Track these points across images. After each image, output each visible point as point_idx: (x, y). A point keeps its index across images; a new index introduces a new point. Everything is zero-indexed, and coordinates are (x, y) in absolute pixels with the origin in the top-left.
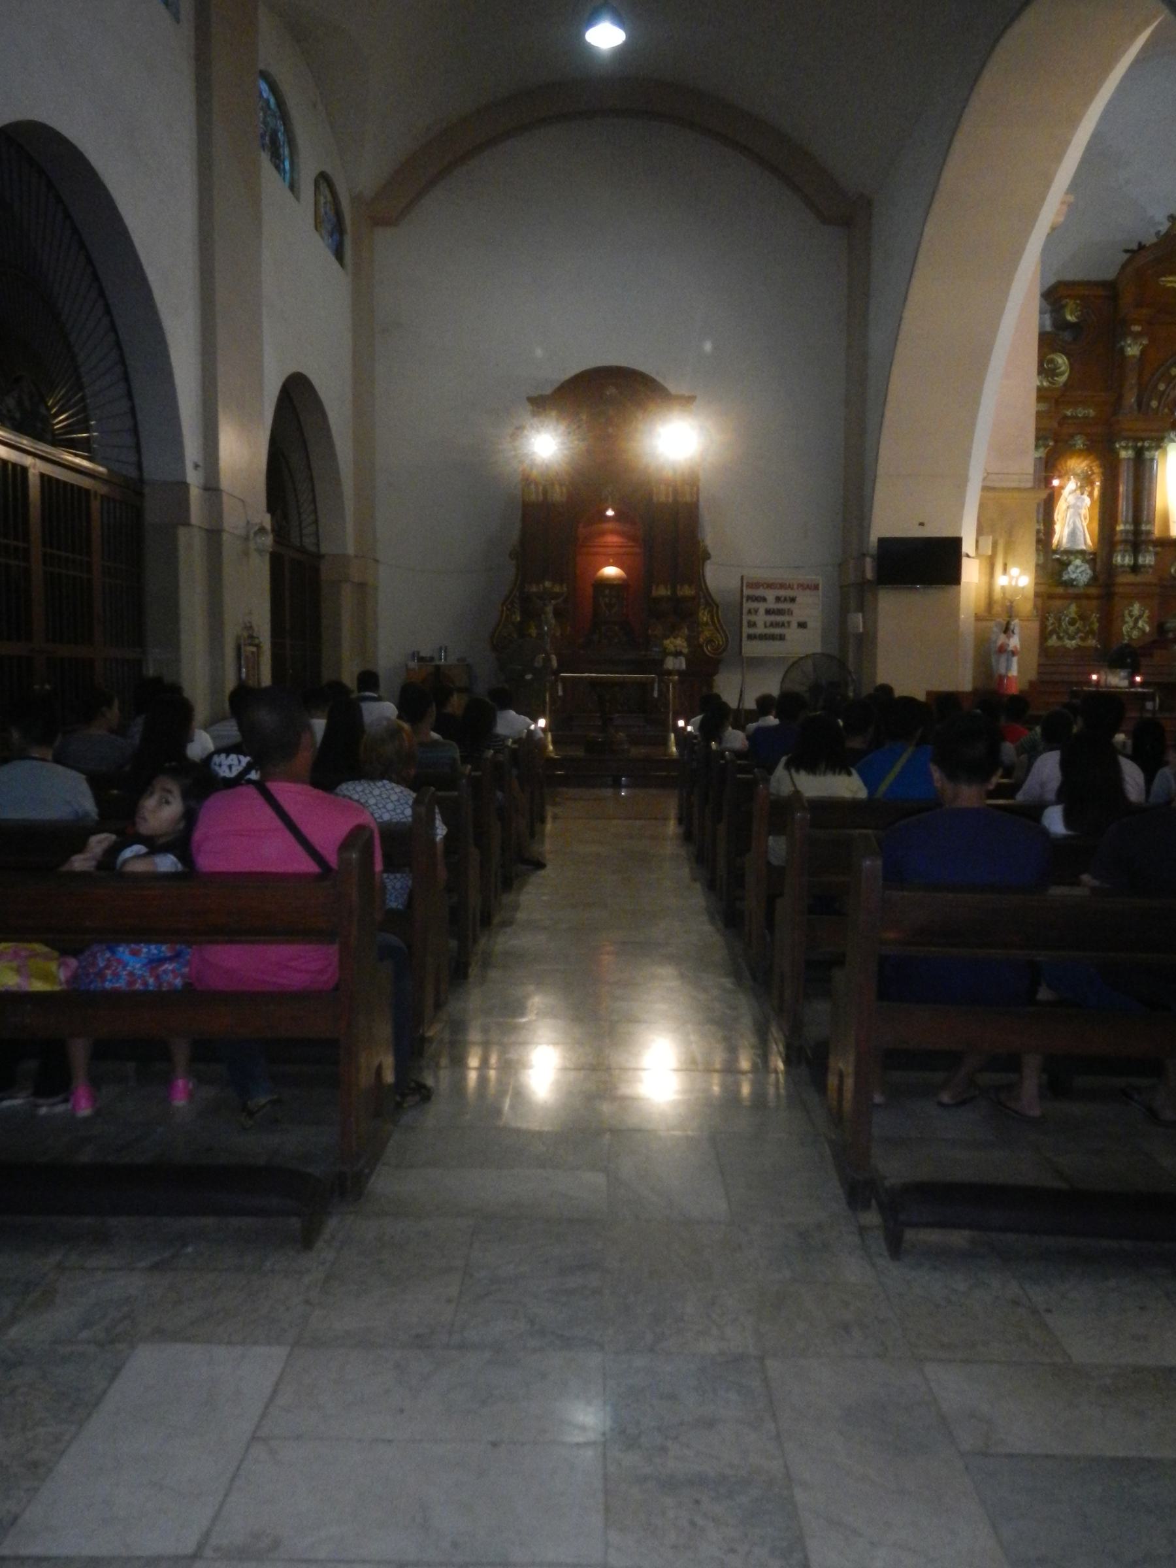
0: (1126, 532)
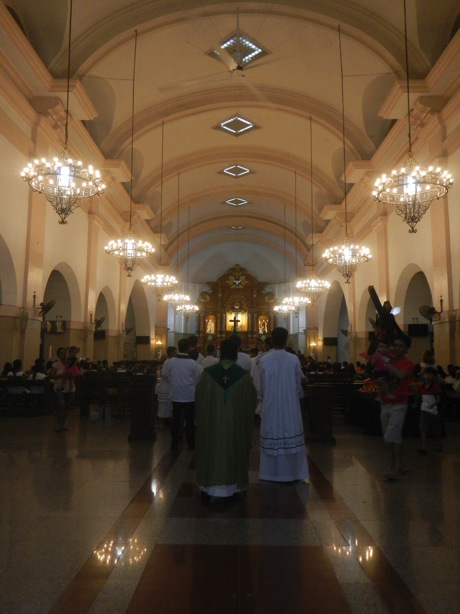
0: (219, 330)
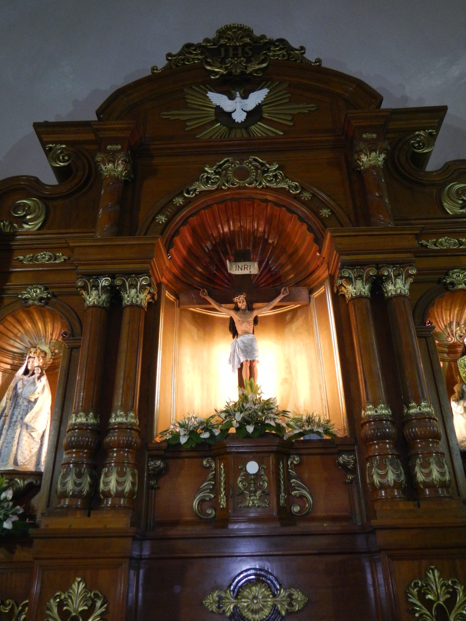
0: (81, 427)
